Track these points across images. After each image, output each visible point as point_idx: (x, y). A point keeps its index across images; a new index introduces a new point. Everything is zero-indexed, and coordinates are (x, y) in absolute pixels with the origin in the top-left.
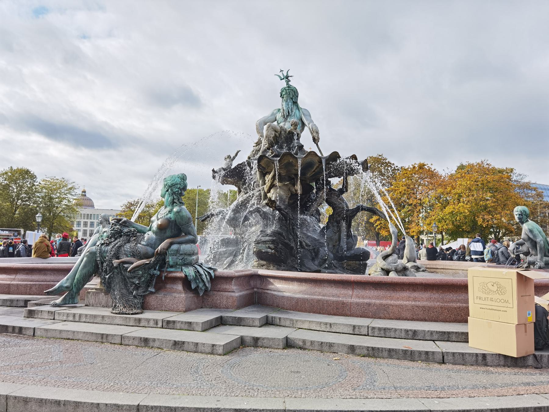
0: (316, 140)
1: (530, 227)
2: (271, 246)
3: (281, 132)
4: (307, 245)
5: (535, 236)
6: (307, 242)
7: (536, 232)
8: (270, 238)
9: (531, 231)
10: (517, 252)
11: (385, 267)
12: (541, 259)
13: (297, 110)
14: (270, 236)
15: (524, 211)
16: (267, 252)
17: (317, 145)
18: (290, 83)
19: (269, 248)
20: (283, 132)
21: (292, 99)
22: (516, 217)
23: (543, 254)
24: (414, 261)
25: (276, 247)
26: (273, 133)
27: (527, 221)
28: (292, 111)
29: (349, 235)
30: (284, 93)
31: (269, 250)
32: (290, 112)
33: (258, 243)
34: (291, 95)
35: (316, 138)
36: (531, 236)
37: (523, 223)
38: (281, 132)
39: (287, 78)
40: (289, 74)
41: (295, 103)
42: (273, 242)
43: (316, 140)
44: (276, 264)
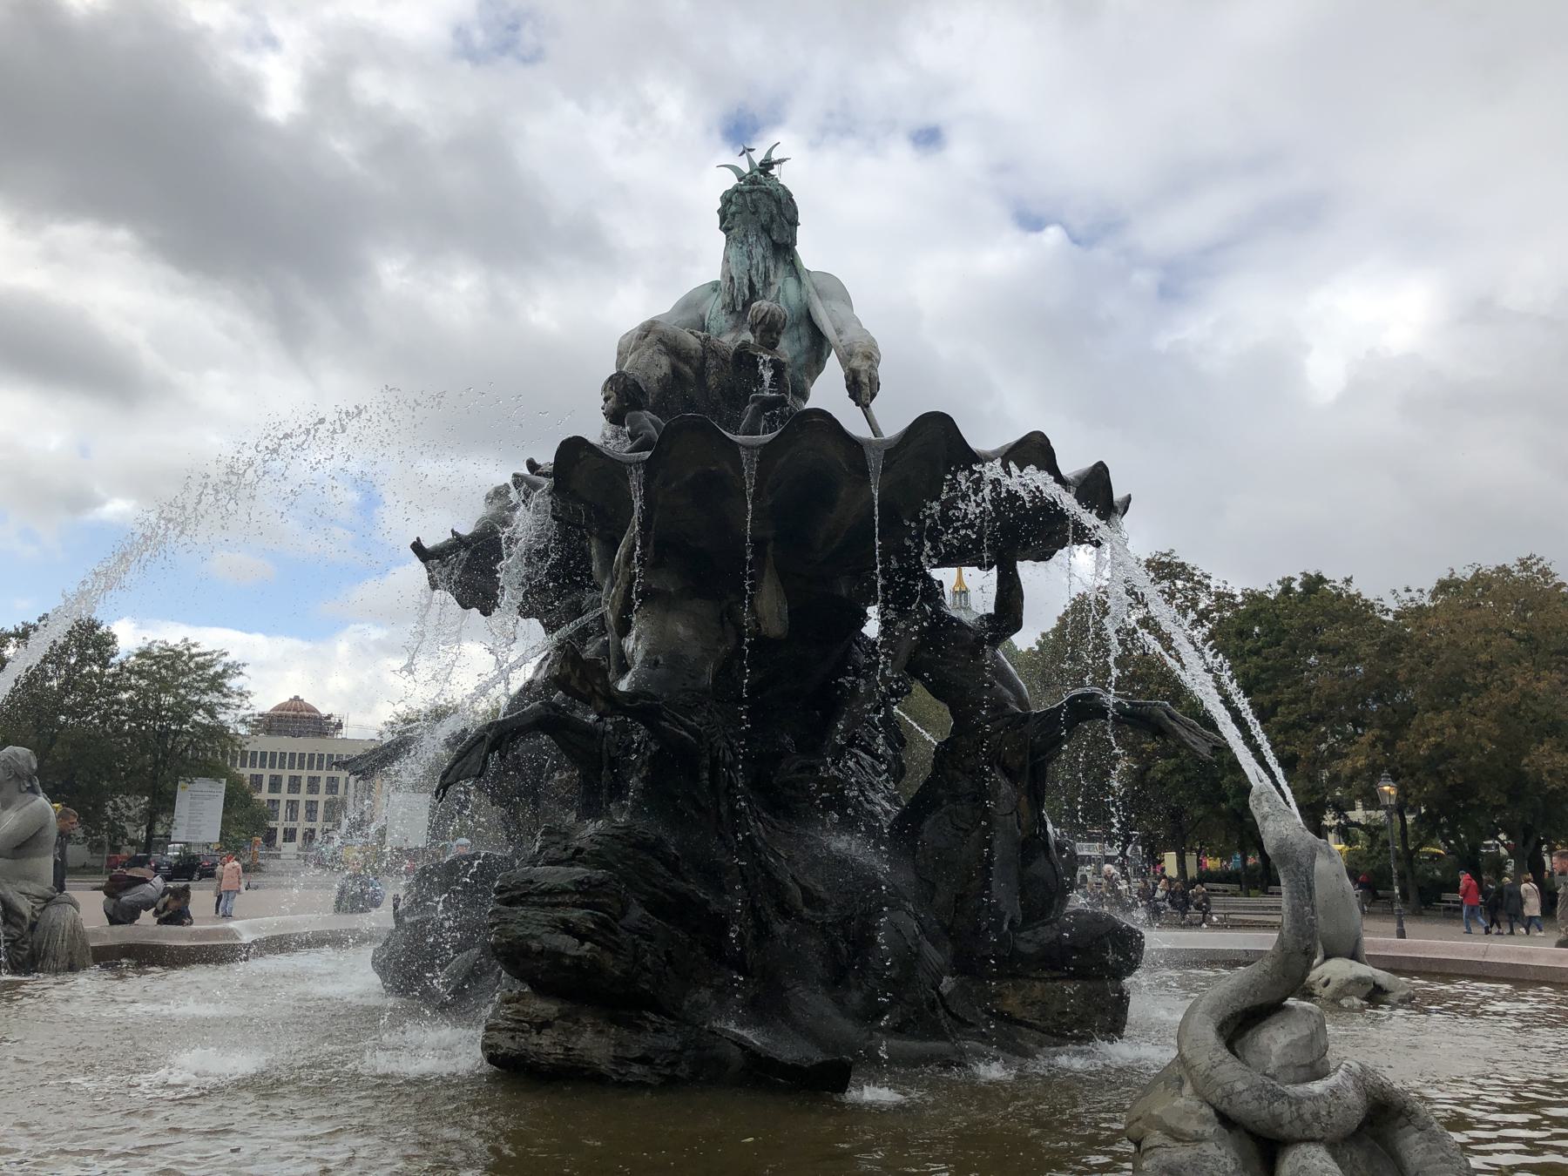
0: (861, 388)
2: (575, 915)
3: (704, 358)
4: (810, 898)
6: (809, 881)
8: (579, 872)
11: (1247, 1106)
14: (596, 860)
16: (557, 955)
17: (866, 408)
19: (568, 928)
20: (711, 363)
21: (766, 230)
24: (1354, 956)
25: (602, 924)
26: (665, 361)
28: (767, 284)
29: (1034, 844)
30: (733, 208)
31: (567, 944)
32: (759, 286)
33: (509, 902)
40: (775, 156)
41: (784, 250)
42: (586, 892)
43: (861, 388)
44: (613, 1021)
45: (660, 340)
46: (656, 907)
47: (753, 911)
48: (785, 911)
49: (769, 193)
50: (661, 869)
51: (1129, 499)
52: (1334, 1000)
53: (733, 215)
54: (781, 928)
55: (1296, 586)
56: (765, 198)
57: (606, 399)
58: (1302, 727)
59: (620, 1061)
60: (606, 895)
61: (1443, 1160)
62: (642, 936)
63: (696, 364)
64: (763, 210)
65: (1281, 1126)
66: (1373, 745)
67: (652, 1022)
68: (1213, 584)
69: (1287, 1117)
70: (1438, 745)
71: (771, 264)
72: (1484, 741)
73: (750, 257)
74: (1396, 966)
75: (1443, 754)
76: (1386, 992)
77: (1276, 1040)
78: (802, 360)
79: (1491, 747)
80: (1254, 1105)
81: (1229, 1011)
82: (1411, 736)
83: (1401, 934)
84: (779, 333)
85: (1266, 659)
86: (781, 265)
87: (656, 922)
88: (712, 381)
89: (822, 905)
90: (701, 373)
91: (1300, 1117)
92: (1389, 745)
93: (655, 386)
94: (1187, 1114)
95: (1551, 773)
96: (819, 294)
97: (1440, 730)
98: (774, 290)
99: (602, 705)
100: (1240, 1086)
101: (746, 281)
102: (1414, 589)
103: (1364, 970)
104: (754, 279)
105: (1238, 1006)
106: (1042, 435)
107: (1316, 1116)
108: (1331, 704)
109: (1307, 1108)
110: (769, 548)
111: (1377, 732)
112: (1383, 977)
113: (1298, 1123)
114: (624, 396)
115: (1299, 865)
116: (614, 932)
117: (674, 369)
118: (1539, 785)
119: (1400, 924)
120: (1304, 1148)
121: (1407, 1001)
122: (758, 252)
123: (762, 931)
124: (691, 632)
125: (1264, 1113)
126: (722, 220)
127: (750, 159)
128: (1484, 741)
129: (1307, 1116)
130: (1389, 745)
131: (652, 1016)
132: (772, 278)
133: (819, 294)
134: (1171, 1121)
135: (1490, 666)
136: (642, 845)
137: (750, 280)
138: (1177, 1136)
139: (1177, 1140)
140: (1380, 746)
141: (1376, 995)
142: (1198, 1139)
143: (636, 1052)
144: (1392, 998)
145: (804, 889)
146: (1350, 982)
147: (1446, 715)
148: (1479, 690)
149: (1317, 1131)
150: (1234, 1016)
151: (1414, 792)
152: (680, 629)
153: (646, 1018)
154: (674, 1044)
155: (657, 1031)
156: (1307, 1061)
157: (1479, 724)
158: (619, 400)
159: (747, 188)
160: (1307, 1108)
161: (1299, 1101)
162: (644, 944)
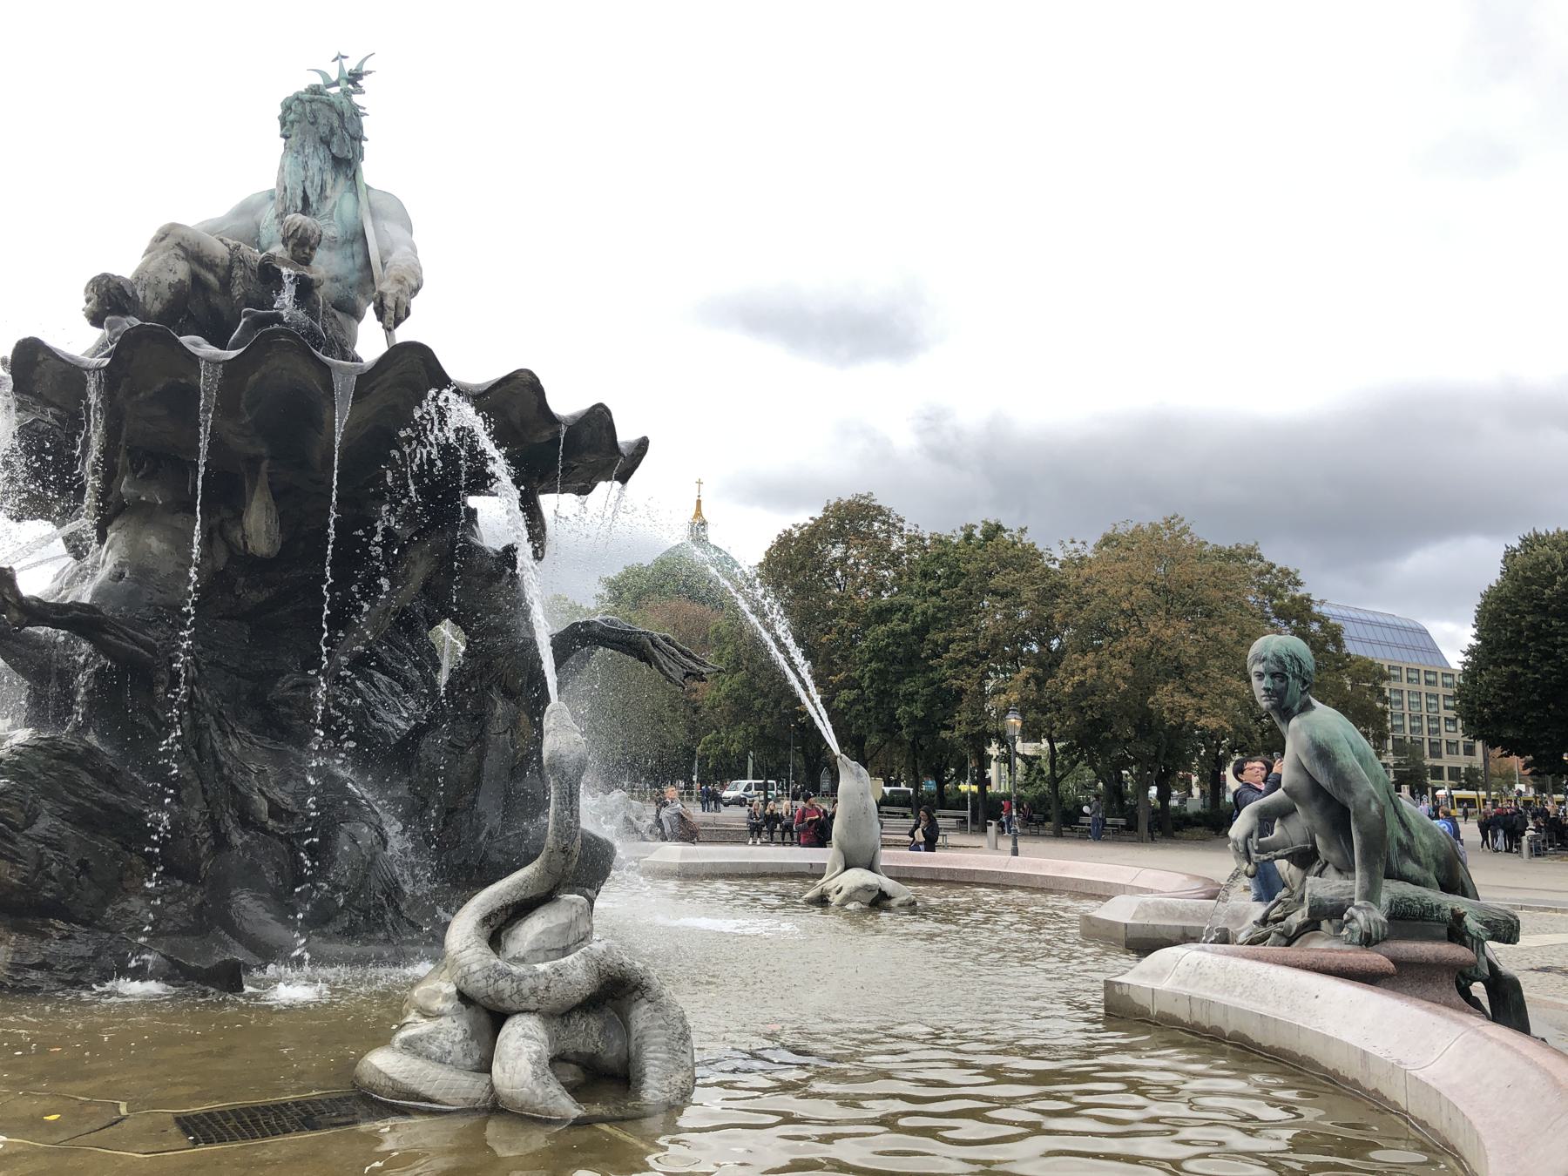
1: (1320, 735)
3: (230, 268)
4: (276, 811)
5: (1340, 777)
6: (278, 794)
7: (1347, 760)
9: (1323, 754)
10: (1262, 849)
11: (477, 985)
12: (1370, 895)
13: (349, 197)
15: (1295, 658)
18: (356, 99)
21: (326, 142)
22: (1259, 687)
23: (1381, 869)
24: (871, 867)
27: (1307, 707)
28: (322, 197)
30: (292, 117)
32: (313, 198)
34: (325, 128)
35: (389, 302)
36: (1324, 780)
37: (1287, 714)
38: (230, 268)
39: (354, 83)
41: (346, 164)
43: (392, 315)
45: (179, 244)
46: (83, 819)
47: (214, 824)
48: (246, 821)
49: (331, 105)
50: (87, 779)
51: (642, 446)
52: (842, 905)
53: (292, 123)
54: (237, 839)
55: (977, 533)
56: (326, 110)
57: (88, 301)
58: (969, 663)
59: (16, 967)
60: (8, 805)
61: (661, 1027)
62: (48, 845)
63: (221, 273)
64: (322, 121)
65: (502, 1000)
66: (1027, 681)
67: (58, 930)
68: (906, 527)
69: (507, 993)
70: (1082, 683)
71: (329, 177)
72: (1119, 681)
73: (305, 167)
74: (904, 876)
75: (1083, 690)
76: (890, 898)
77: (533, 929)
78: (354, 278)
79: (1124, 687)
80: (483, 983)
81: (501, 903)
82: (1061, 674)
83: (1015, 852)
84: (313, 249)
85: (945, 600)
86: (341, 180)
87: (68, 831)
88: (237, 291)
89: (292, 815)
90: (226, 283)
91: (519, 991)
92: (1040, 682)
93: (167, 294)
94: (437, 993)
95: (1171, 710)
96: (374, 214)
97: (1084, 670)
98: (330, 203)
99: (16, 615)
100: (475, 967)
101: (299, 192)
102: (1078, 541)
103: (868, 878)
104: (309, 192)
105: (508, 899)
106: (531, 373)
107: (534, 991)
108: (995, 642)
109: (526, 986)
110: (264, 465)
111: (1031, 670)
112: (888, 884)
113: (516, 998)
114: (109, 299)
115: (565, 773)
116: (13, 842)
117: (195, 278)
118: (1162, 721)
119: (1015, 843)
120: (518, 1018)
121: (911, 906)
122: (315, 163)
123: (221, 842)
124: (165, 546)
125: (491, 992)
126: (283, 125)
127: (341, 65)
128: (1119, 681)
129: (526, 991)
130: (1040, 682)
131: (59, 924)
132: (328, 192)
133: (374, 214)
134: (421, 1001)
135: (1129, 614)
136: (67, 756)
137: (304, 191)
138: (426, 1014)
139: (425, 1017)
140: (1032, 684)
141: (879, 901)
142: (440, 1015)
143: (36, 958)
144: (894, 903)
145: (270, 800)
146: (858, 889)
147: (1091, 656)
148: (1116, 636)
149: (532, 1003)
150: (505, 908)
151: (1058, 724)
152: (155, 543)
153: (53, 926)
154: (86, 950)
155: (63, 938)
156: (561, 945)
157: (1117, 665)
158: (100, 303)
159: (307, 96)
160: (526, 986)
161: (521, 978)
162: (50, 854)
